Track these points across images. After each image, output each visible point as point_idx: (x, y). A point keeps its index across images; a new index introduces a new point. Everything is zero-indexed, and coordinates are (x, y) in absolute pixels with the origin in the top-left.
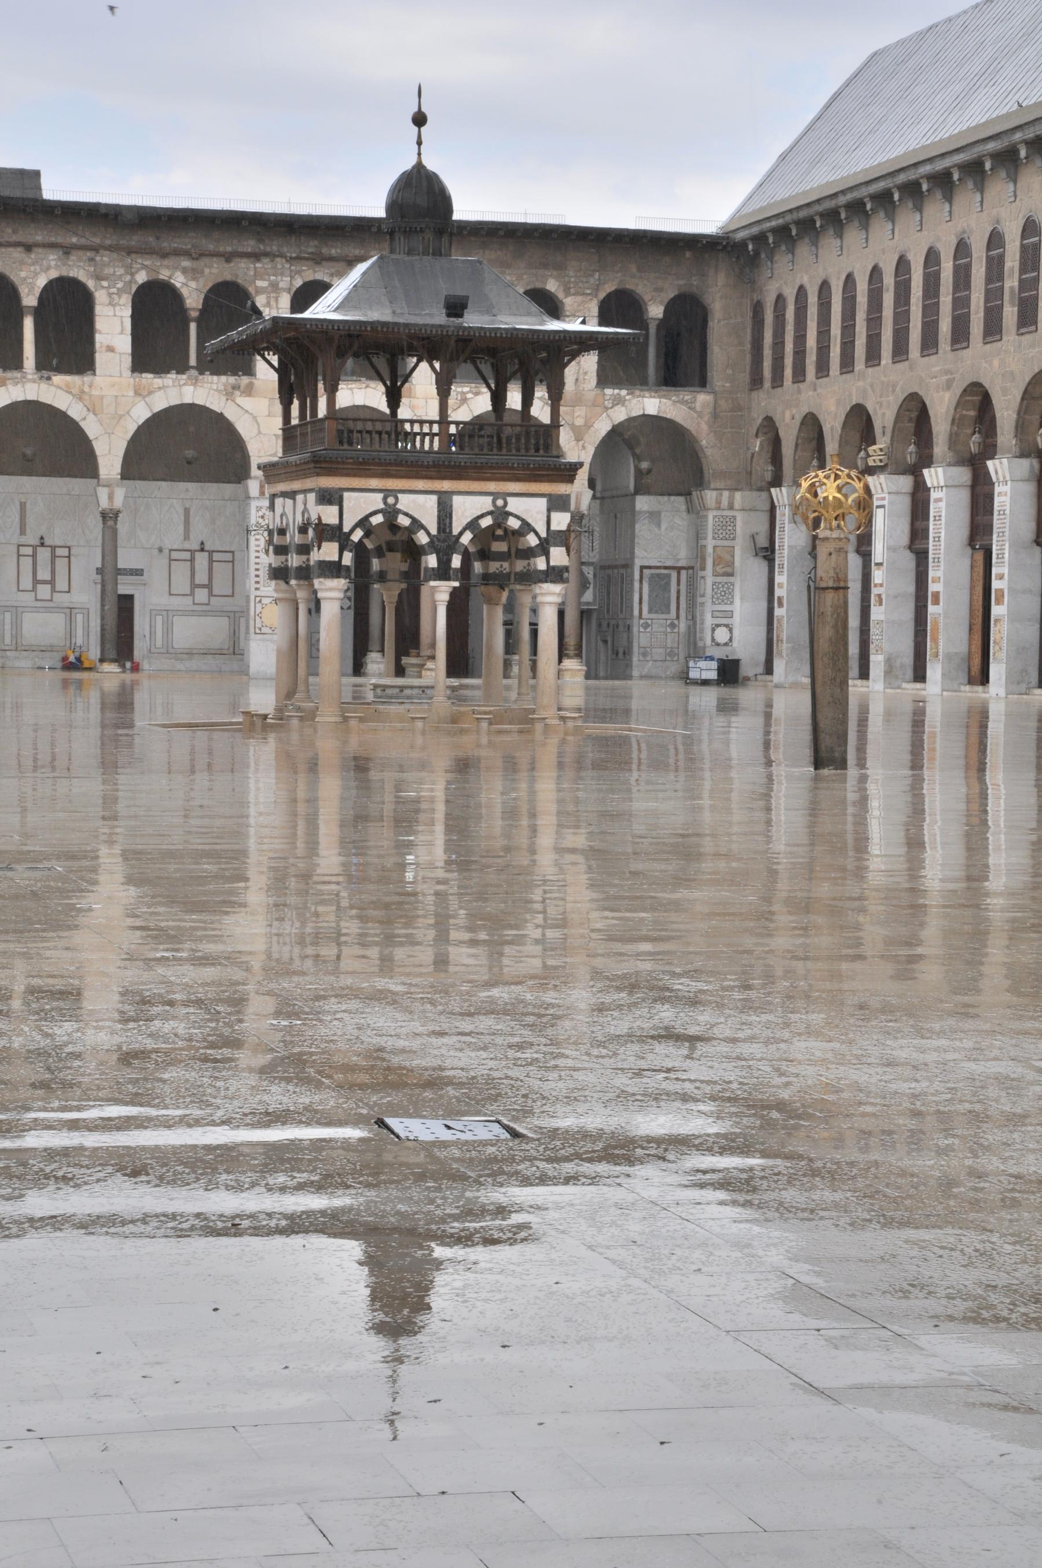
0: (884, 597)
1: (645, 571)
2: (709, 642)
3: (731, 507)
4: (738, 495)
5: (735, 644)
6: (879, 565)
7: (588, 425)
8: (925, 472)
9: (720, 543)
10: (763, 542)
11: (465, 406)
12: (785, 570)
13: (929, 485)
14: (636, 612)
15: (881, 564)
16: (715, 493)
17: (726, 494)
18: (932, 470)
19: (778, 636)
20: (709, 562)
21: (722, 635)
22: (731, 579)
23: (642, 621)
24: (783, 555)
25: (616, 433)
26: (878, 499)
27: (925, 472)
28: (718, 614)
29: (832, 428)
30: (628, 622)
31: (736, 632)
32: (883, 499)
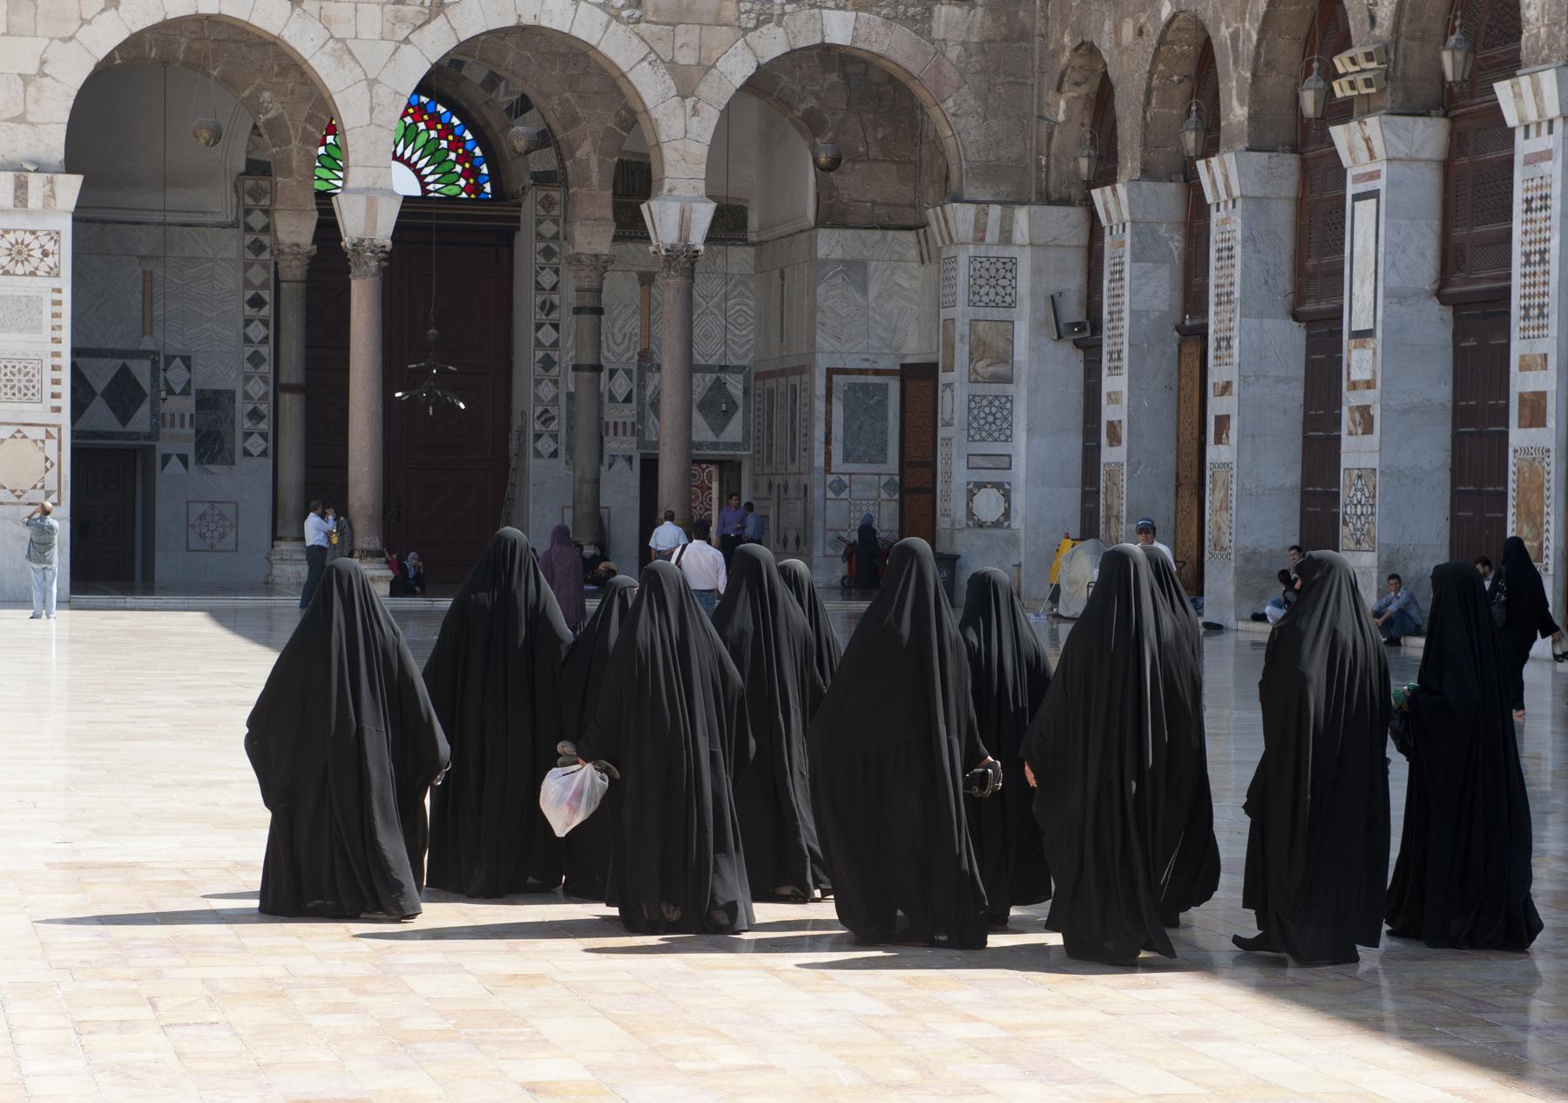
0: (1376, 412)
1: (835, 377)
2: (960, 513)
3: (1006, 238)
4: (1022, 215)
5: (1017, 522)
6: (1363, 335)
7: (705, 68)
8: (1502, 89)
9: (982, 313)
10: (1073, 311)
11: (441, 20)
12: (1125, 363)
13: (1511, 119)
14: (819, 461)
15: (1369, 333)
16: (970, 210)
17: (995, 211)
18: (1524, 81)
19: (1109, 507)
20: (962, 352)
21: (988, 505)
22: (1009, 389)
23: (830, 478)
24: (1118, 334)
25: (761, 83)
26: (1357, 179)
27: (1502, 89)
28: (979, 461)
29: (1235, 36)
30: (805, 480)
31: (1018, 500)
32: (1374, 175)
